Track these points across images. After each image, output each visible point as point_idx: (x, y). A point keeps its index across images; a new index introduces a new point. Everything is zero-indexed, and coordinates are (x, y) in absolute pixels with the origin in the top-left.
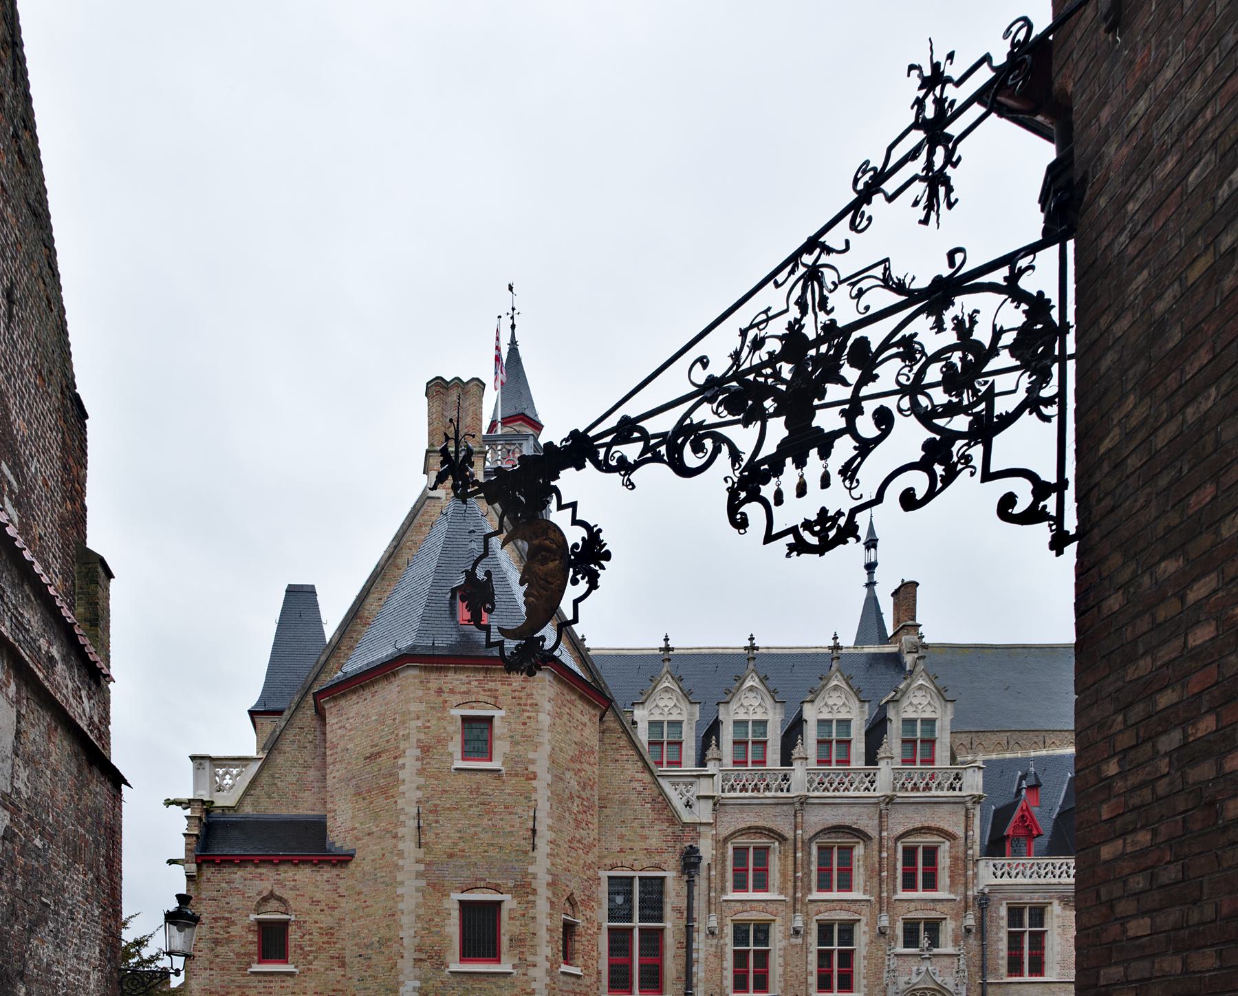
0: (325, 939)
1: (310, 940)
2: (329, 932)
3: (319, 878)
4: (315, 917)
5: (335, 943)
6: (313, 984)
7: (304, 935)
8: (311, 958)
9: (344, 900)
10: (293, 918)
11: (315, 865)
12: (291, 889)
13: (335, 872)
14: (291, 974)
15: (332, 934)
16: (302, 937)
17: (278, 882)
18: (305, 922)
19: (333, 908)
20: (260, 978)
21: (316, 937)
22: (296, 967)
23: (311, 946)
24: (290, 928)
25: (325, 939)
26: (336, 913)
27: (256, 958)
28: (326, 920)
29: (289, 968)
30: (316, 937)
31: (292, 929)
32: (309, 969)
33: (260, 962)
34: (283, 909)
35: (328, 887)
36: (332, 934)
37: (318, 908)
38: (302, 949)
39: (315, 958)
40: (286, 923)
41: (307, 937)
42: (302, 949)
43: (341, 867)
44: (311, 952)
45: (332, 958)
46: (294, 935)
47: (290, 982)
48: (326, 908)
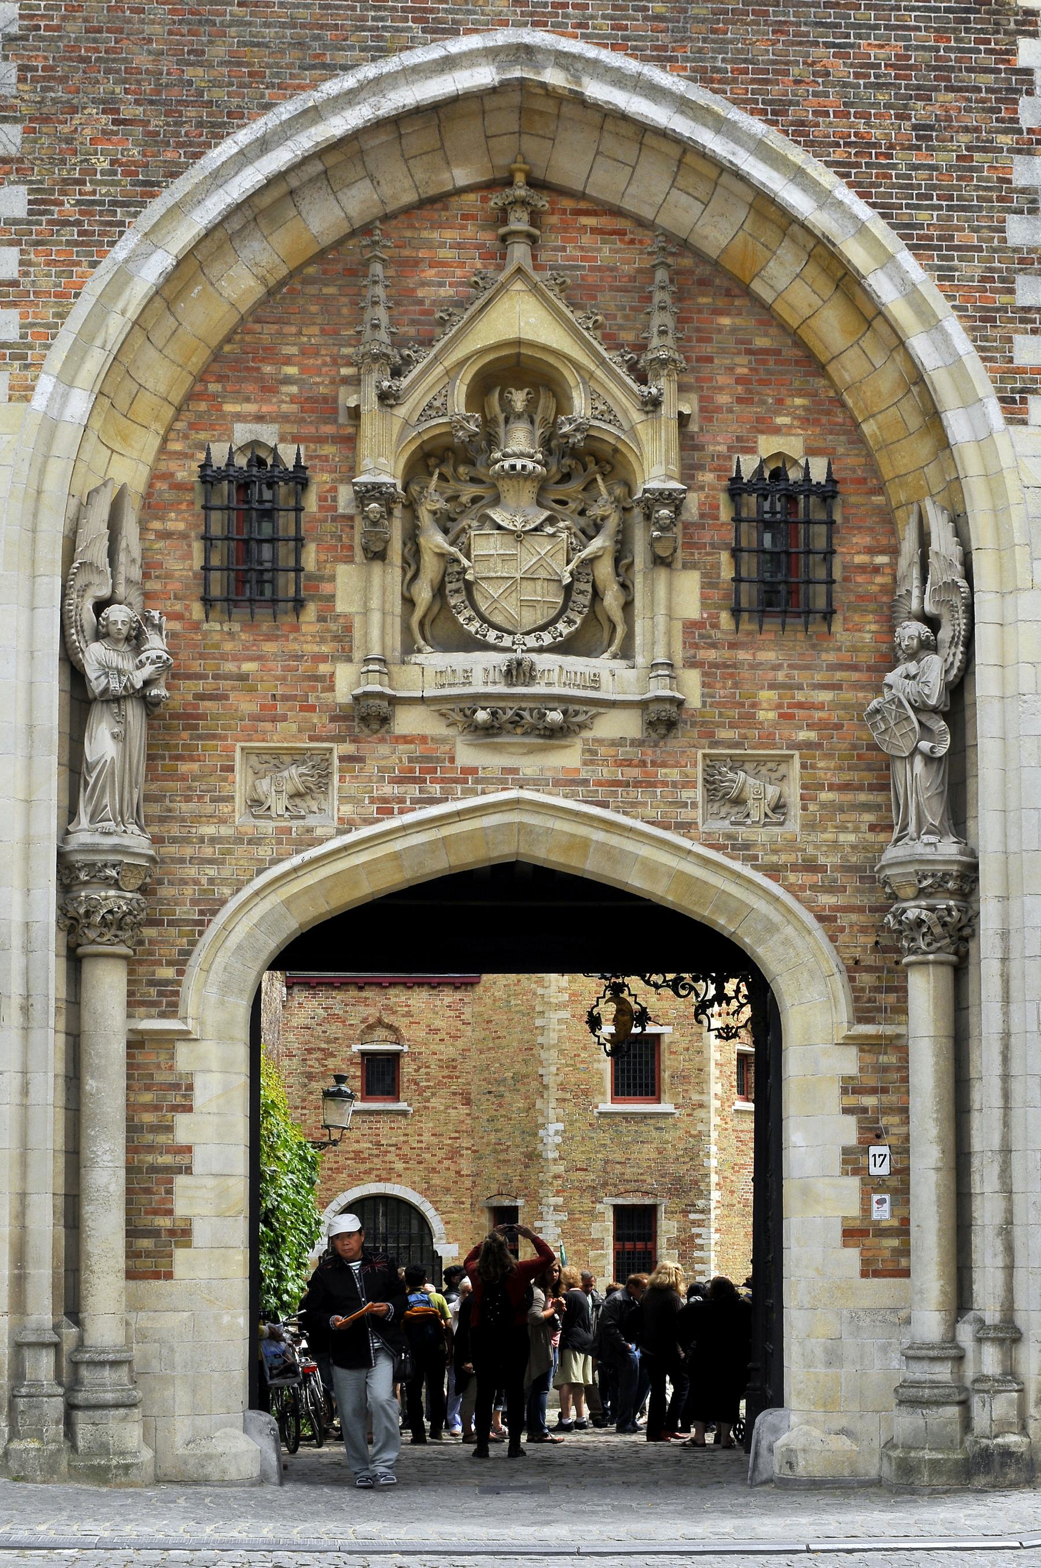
0: (446, 1072)
1: (427, 1074)
2: (451, 1065)
3: (438, 1003)
4: (433, 1047)
5: (457, 1077)
6: (431, 1125)
7: (419, 1068)
8: (428, 1094)
9: (469, 1028)
10: (406, 1049)
11: (434, 988)
12: (403, 1016)
13: (458, 995)
14: (404, 1113)
15: (455, 1067)
16: (417, 1071)
17: (387, 1008)
18: (420, 1053)
19: (455, 1038)
20: (365, 1118)
21: (434, 1070)
22: (410, 1105)
23: (428, 1080)
24: (402, 1061)
25: (446, 1072)
26: (460, 1043)
27: (359, 1094)
28: (448, 1051)
29: (402, 1106)
30: (434, 1070)
31: (405, 1061)
32: (426, 1108)
33: (363, 1100)
34: (393, 1038)
35: (452, 1014)
36: (455, 1067)
37: (437, 1037)
38: (416, 1084)
39: (434, 1094)
40: (396, 1056)
41: (423, 1070)
42: (416, 1084)
43: (466, 990)
44: (428, 1087)
45: (454, 1094)
46: (407, 1069)
47: (403, 1122)
48: (447, 1037)
